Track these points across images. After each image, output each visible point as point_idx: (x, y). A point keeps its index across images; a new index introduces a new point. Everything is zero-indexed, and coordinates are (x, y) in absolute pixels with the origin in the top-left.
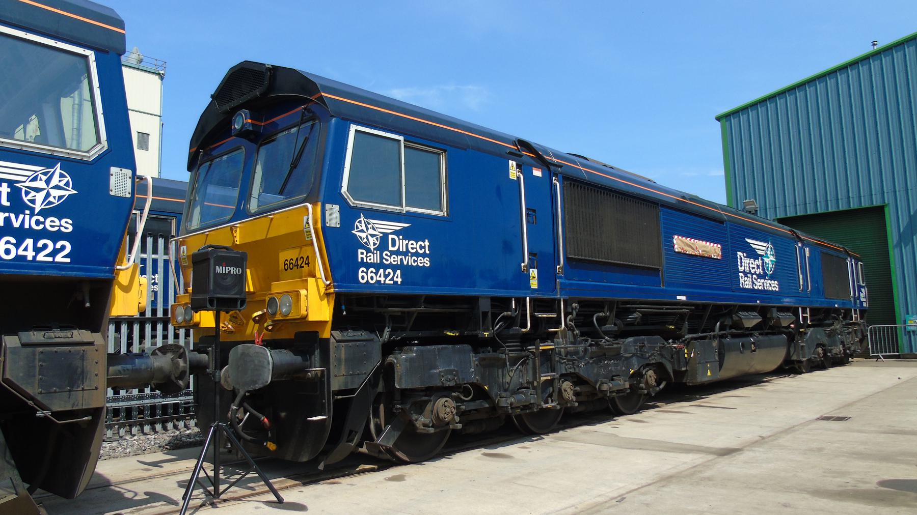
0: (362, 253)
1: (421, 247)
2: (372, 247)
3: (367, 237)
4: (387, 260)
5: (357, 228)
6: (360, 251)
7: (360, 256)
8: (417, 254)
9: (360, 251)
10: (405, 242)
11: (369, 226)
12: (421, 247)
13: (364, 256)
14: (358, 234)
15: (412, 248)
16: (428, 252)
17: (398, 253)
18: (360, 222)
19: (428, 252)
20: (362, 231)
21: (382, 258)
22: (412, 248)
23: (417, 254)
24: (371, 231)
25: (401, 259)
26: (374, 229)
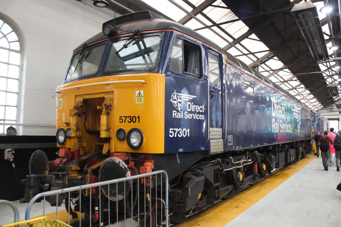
0: (175, 113)
1: (201, 109)
2: (179, 109)
3: (177, 103)
4: (186, 116)
5: (173, 98)
6: (174, 111)
7: (174, 114)
8: (199, 113)
9: (174, 111)
10: (195, 106)
11: (178, 97)
12: (201, 109)
13: (175, 114)
14: (173, 101)
15: (197, 110)
16: (204, 112)
17: (191, 112)
18: (174, 95)
19: (204, 112)
20: (175, 100)
21: (184, 115)
22: (197, 110)
23: (199, 113)
24: (179, 100)
25: (193, 116)
26: (181, 99)
